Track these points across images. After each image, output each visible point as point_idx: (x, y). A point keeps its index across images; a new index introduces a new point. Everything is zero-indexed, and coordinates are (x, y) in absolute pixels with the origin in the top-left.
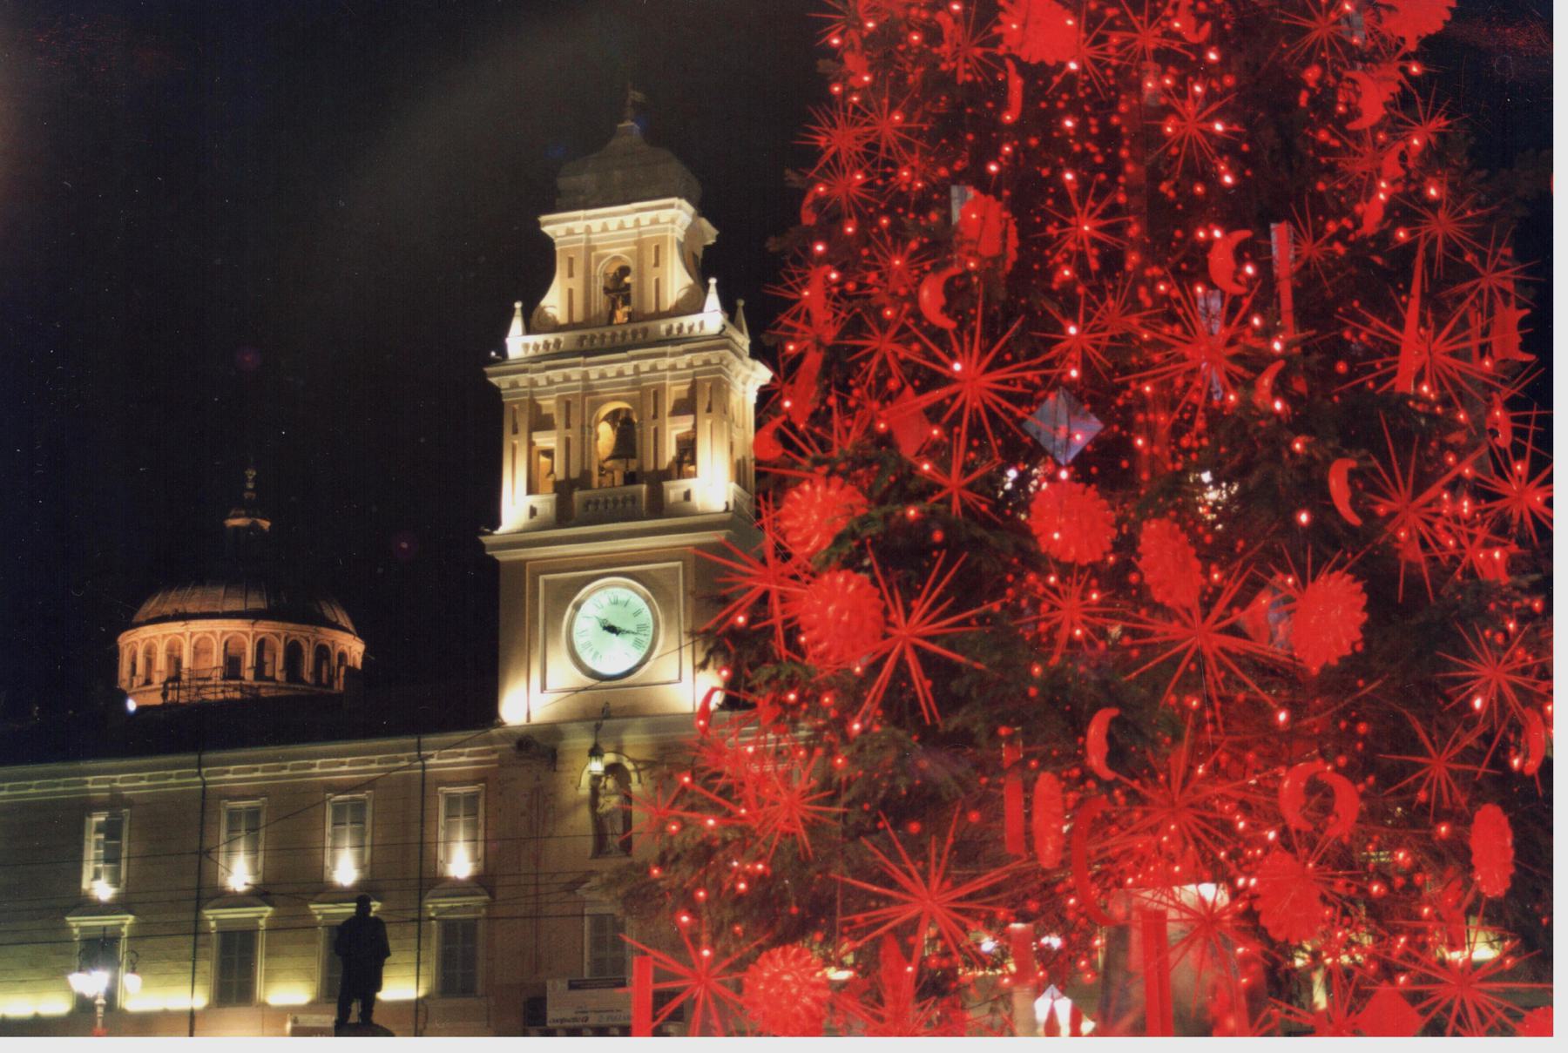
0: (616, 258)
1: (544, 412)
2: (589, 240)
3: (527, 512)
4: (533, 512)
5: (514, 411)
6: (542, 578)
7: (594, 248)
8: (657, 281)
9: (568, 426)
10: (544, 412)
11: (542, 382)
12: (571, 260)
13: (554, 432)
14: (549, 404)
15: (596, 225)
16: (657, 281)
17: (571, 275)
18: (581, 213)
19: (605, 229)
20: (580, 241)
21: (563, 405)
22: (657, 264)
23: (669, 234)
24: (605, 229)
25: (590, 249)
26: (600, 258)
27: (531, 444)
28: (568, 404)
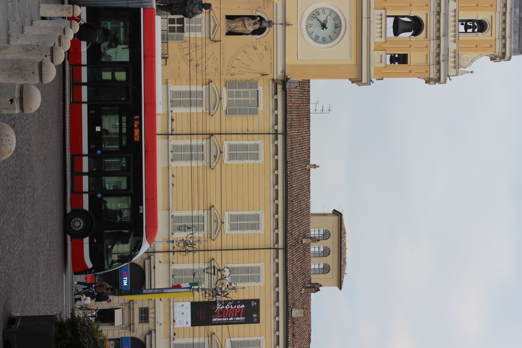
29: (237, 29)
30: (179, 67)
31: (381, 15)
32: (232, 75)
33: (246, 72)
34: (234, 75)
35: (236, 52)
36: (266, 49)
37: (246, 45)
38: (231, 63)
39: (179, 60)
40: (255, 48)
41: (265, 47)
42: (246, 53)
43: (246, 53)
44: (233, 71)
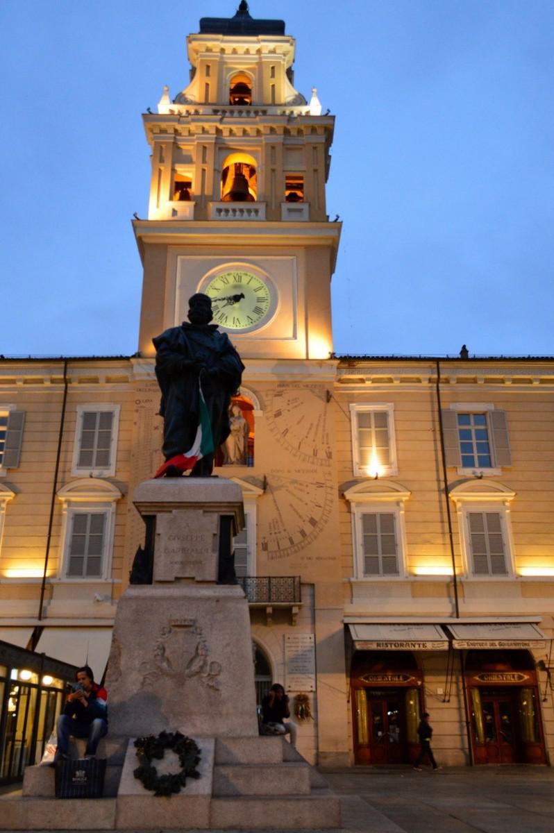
0: (242, 73)
1: (184, 153)
2: (222, 58)
3: (171, 212)
4: (174, 212)
5: (161, 148)
6: (179, 258)
7: (226, 63)
8: (273, 86)
9: (204, 161)
10: (184, 153)
11: (185, 133)
12: (208, 67)
13: (194, 166)
14: (189, 148)
15: (229, 47)
16: (273, 86)
17: (208, 74)
18: (220, 37)
19: (235, 51)
20: (217, 56)
21: (201, 149)
22: (273, 76)
23: (282, 62)
24: (235, 51)
25: (222, 63)
26: (231, 69)
27: (173, 171)
28: (205, 148)
29: (242, 449)
30: (318, 558)
31: (219, 211)
32: (329, 456)
33: (324, 430)
34: (330, 453)
35: (286, 449)
36: (279, 394)
37: (272, 430)
38: (307, 458)
39: (303, 558)
40: (278, 414)
41: (276, 396)
42: (287, 431)
43: (287, 431)
44: (322, 455)
